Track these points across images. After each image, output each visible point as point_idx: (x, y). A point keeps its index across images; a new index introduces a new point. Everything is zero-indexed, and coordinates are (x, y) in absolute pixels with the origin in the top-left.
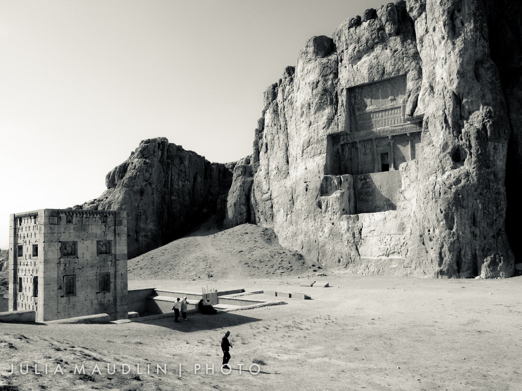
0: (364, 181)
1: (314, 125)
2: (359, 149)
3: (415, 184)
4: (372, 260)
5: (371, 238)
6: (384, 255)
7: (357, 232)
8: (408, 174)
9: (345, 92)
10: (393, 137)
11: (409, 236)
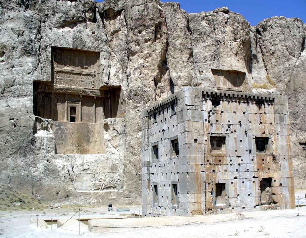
0: (58, 127)
1: (18, 69)
2: (52, 99)
3: (122, 135)
4: (89, 194)
6: (99, 189)
7: (70, 169)
9: (50, 49)
10: (83, 96)
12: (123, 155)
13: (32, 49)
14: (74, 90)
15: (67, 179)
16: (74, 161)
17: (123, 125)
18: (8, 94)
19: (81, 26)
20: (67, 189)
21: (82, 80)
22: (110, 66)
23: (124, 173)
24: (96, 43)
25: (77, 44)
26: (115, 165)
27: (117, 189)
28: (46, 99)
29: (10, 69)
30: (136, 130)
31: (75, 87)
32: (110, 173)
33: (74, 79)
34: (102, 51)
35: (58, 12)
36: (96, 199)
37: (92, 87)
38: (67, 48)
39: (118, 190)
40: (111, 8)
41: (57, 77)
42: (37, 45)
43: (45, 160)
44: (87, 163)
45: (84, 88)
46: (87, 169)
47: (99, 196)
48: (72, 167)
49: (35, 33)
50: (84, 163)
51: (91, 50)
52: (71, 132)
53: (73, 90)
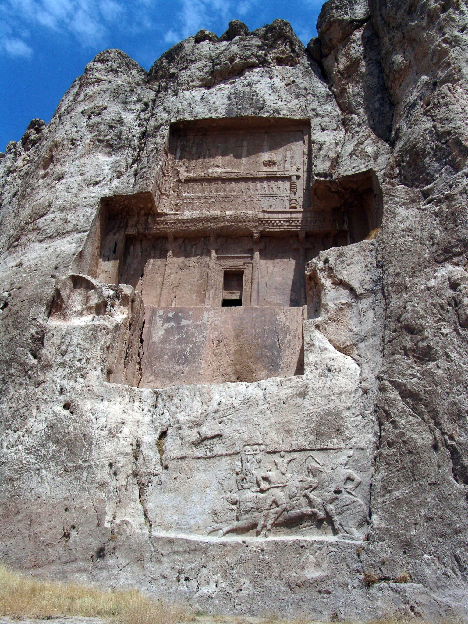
0: (172, 324)
1: (72, 179)
3: (371, 300)
9: (166, 131)
10: (264, 235)
13: (117, 136)
16: (174, 409)
18: (30, 236)
19: (255, 74)
20: (108, 518)
21: (257, 193)
22: (340, 145)
24: (295, 101)
25: (240, 107)
26: (337, 415)
27: (335, 532)
30: (427, 264)
31: (238, 211)
32: (312, 453)
33: (233, 194)
34: (317, 115)
35: (196, 60)
36: (226, 576)
38: (211, 120)
39: (340, 534)
40: (334, 21)
41: (186, 194)
42: (137, 131)
44: (217, 411)
45: (264, 212)
46: (213, 437)
47: (244, 561)
48: (160, 431)
51: (280, 116)
53: (228, 221)
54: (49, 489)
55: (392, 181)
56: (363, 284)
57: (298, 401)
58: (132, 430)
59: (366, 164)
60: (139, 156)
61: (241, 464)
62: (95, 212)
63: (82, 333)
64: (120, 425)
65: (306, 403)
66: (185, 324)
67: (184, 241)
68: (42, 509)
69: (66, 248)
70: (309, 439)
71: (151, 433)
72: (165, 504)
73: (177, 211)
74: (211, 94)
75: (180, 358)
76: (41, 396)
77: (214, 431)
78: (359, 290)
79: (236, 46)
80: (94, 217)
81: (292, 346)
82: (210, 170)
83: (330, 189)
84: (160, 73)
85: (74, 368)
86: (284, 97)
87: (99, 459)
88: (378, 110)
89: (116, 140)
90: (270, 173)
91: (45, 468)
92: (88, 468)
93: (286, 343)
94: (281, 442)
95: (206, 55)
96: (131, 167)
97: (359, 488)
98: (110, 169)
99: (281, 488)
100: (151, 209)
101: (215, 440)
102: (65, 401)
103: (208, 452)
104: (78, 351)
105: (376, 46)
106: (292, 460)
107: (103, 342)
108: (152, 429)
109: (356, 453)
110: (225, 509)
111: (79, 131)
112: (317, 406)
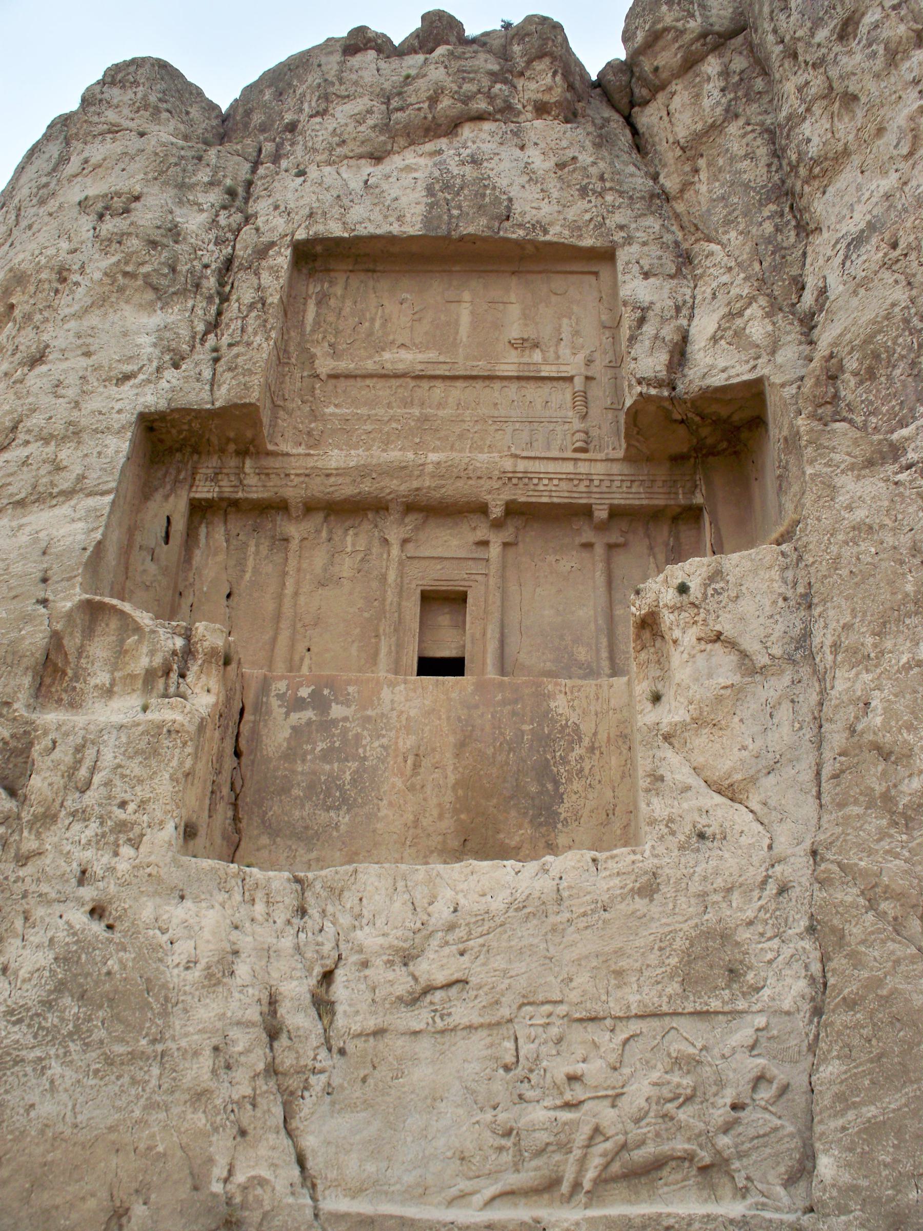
0: (309, 714)
1: (65, 365)
2: (294, 545)
5: (424, 1047)
8: (726, 625)
9: (282, 259)
10: (513, 510)
11: (801, 1022)
12: (807, 845)
14: (442, 472)
15: (241, 1075)
17: (789, 594)
20: (219, 1171)
21: (496, 413)
22: (685, 312)
23: (818, 1012)
24: (582, 204)
25: (455, 212)
28: (252, 549)
29: (19, 372)
34: (629, 240)
35: (348, 96)
37: (576, 450)
38: (391, 239)
39: (750, 1201)
41: (331, 409)
42: (214, 256)
43: (81, 902)
44: (451, 927)
48: (318, 970)
49: (205, 206)
50: (431, 934)
51: (548, 238)
52: (407, 742)
54: (70, 1107)
55: (820, 411)
56: (769, 644)
57: (637, 907)
58: (257, 968)
59: (752, 363)
60: (219, 314)
61: (513, 1047)
62: (125, 446)
63: (124, 739)
64: (230, 958)
65: (655, 909)
66: (340, 716)
67: (326, 518)
68: (58, 1154)
69: (62, 532)
70: (669, 990)
71: (299, 974)
72: (344, 1138)
73: (310, 447)
74: (387, 177)
75: (328, 794)
76: (33, 888)
77: (449, 972)
78: (759, 657)
79: (442, 70)
80: (123, 460)
81: (586, 771)
82: (387, 355)
83: (667, 414)
84: (257, 118)
85: (109, 823)
86: (555, 194)
87: (186, 1035)
88: (769, 241)
89: (165, 275)
90: (526, 368)
91: (57, 1056)
92: (162, 1057)
93: (573, 763)
94: (604, 998)
95: (371, 86)
96: (203, 340)
97: (785, 1097)
98: (155, 345)
99: (610, 1100)
100: (252, 441)
101: (454, 991)
102: (93, 900)
103: (438, 1020)
104: (117, 782)
105: (759, 93)
106: (632, 1036)
107: (174, 763)
108: (300, 966)
109: (774, 1021)
110: (486, 1147)
111: (76, 251)
112: (680, 918)
